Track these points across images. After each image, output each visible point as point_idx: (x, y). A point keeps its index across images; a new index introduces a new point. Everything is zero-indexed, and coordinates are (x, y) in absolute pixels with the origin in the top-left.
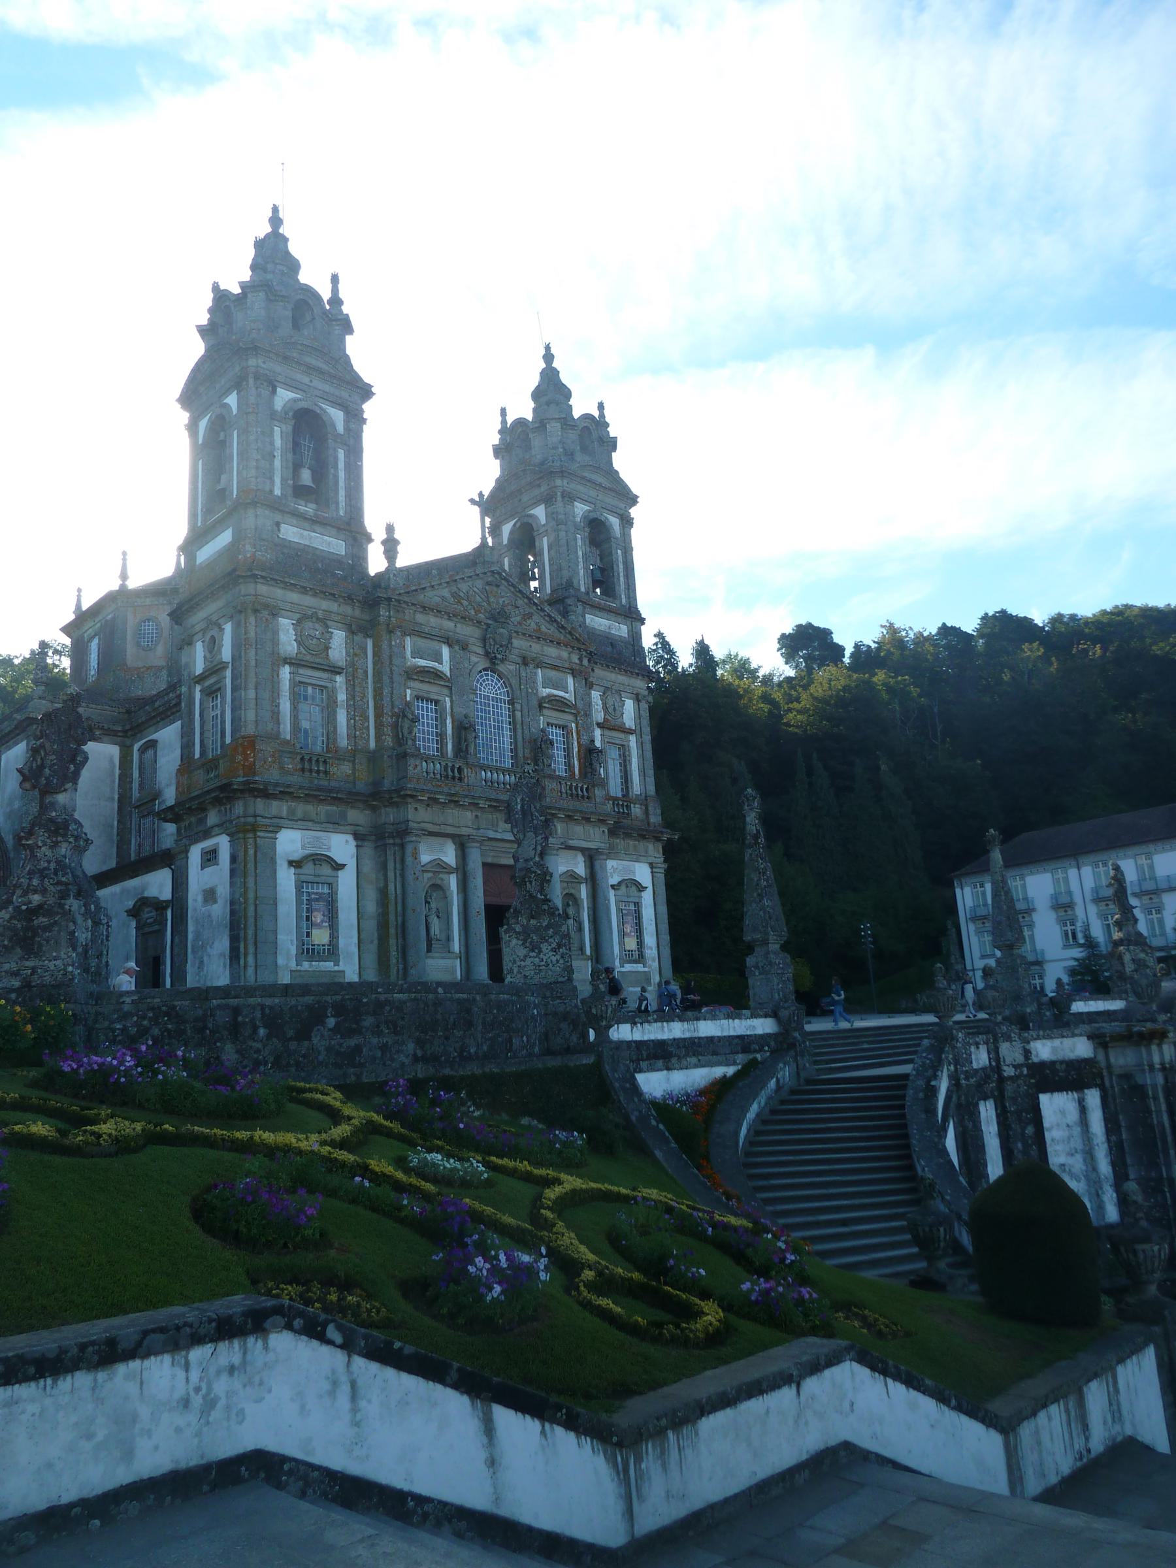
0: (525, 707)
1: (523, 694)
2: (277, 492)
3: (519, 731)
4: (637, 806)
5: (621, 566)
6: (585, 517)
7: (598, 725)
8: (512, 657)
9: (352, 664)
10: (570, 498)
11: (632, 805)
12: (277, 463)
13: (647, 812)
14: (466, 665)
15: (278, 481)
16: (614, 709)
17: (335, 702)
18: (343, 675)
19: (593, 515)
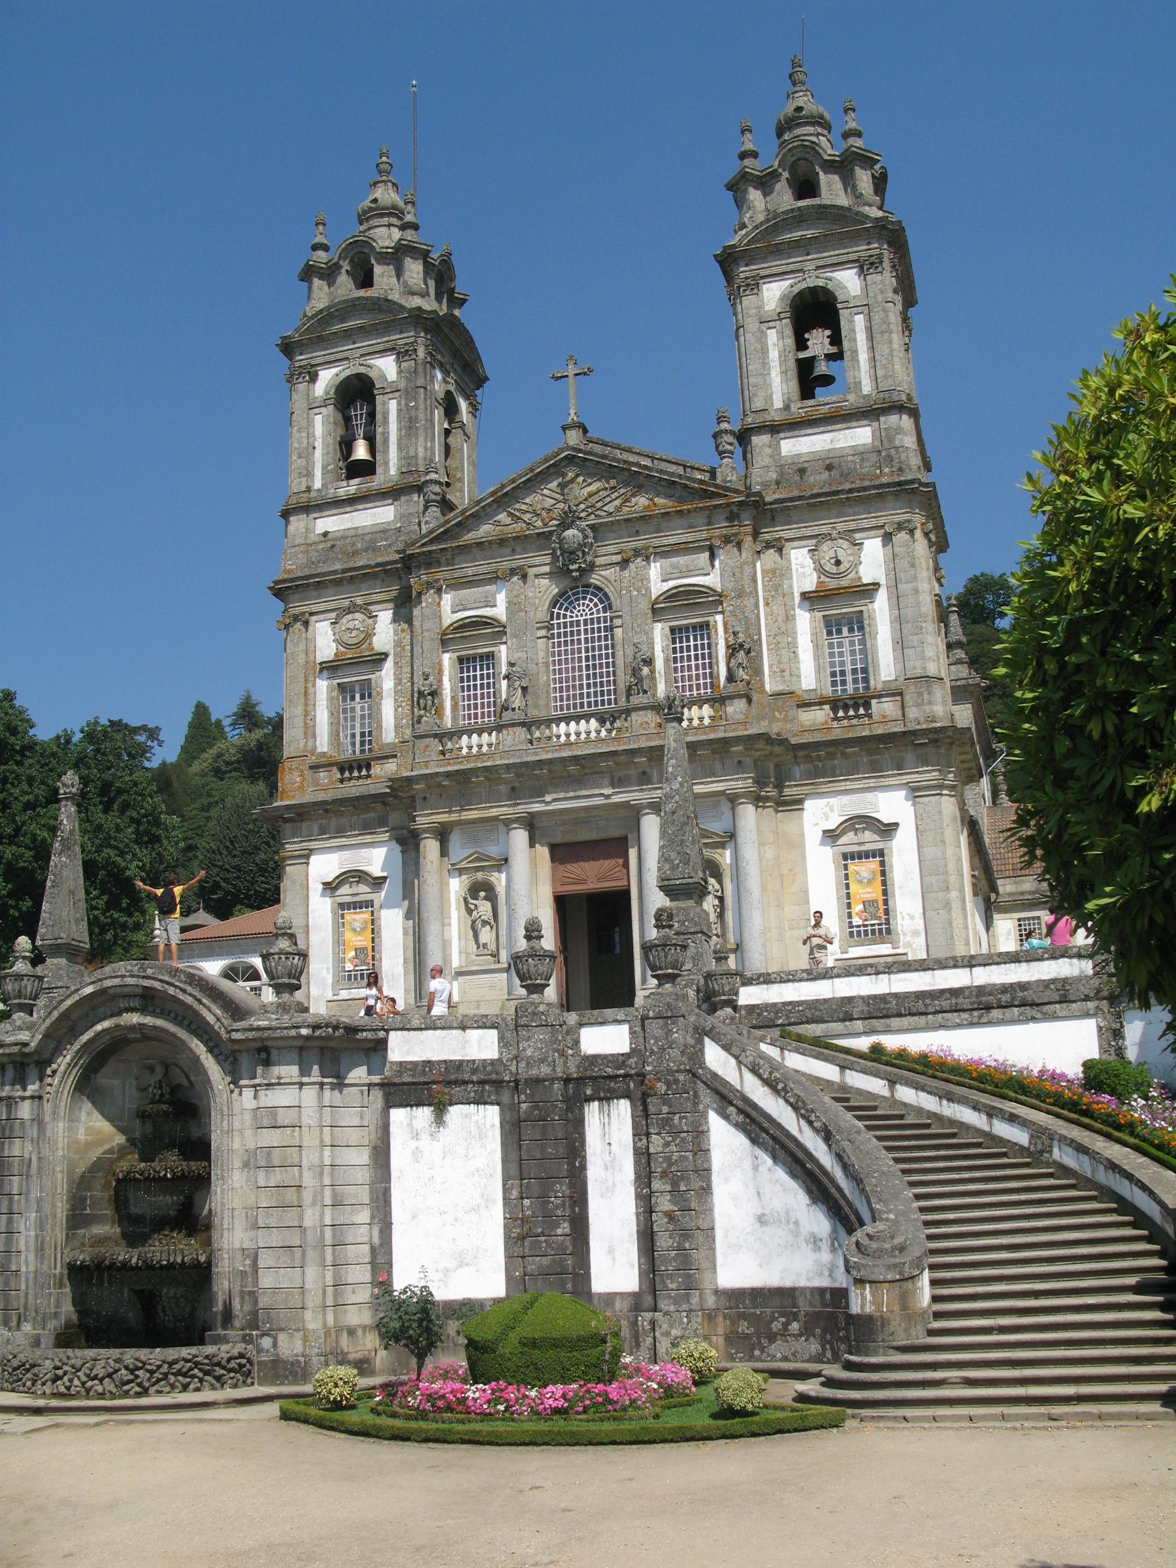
0: (627, 618)
1: (626, 599)
2: (318, 485)
3: (619, 654)
4: (883, 700)
5: (861, 338)
6: (782, 299)
7: (805, 596)
8: (600, 561)
9: (398, 644)
10: (754, 285)
11: (874, 702)
12: (318, 454)
13: (903, 707)
14: (531, 594)
15: (318, 473)
16: (838, 563)
17: (380, 694)
18: (390, 659)
19: (796, 290)
